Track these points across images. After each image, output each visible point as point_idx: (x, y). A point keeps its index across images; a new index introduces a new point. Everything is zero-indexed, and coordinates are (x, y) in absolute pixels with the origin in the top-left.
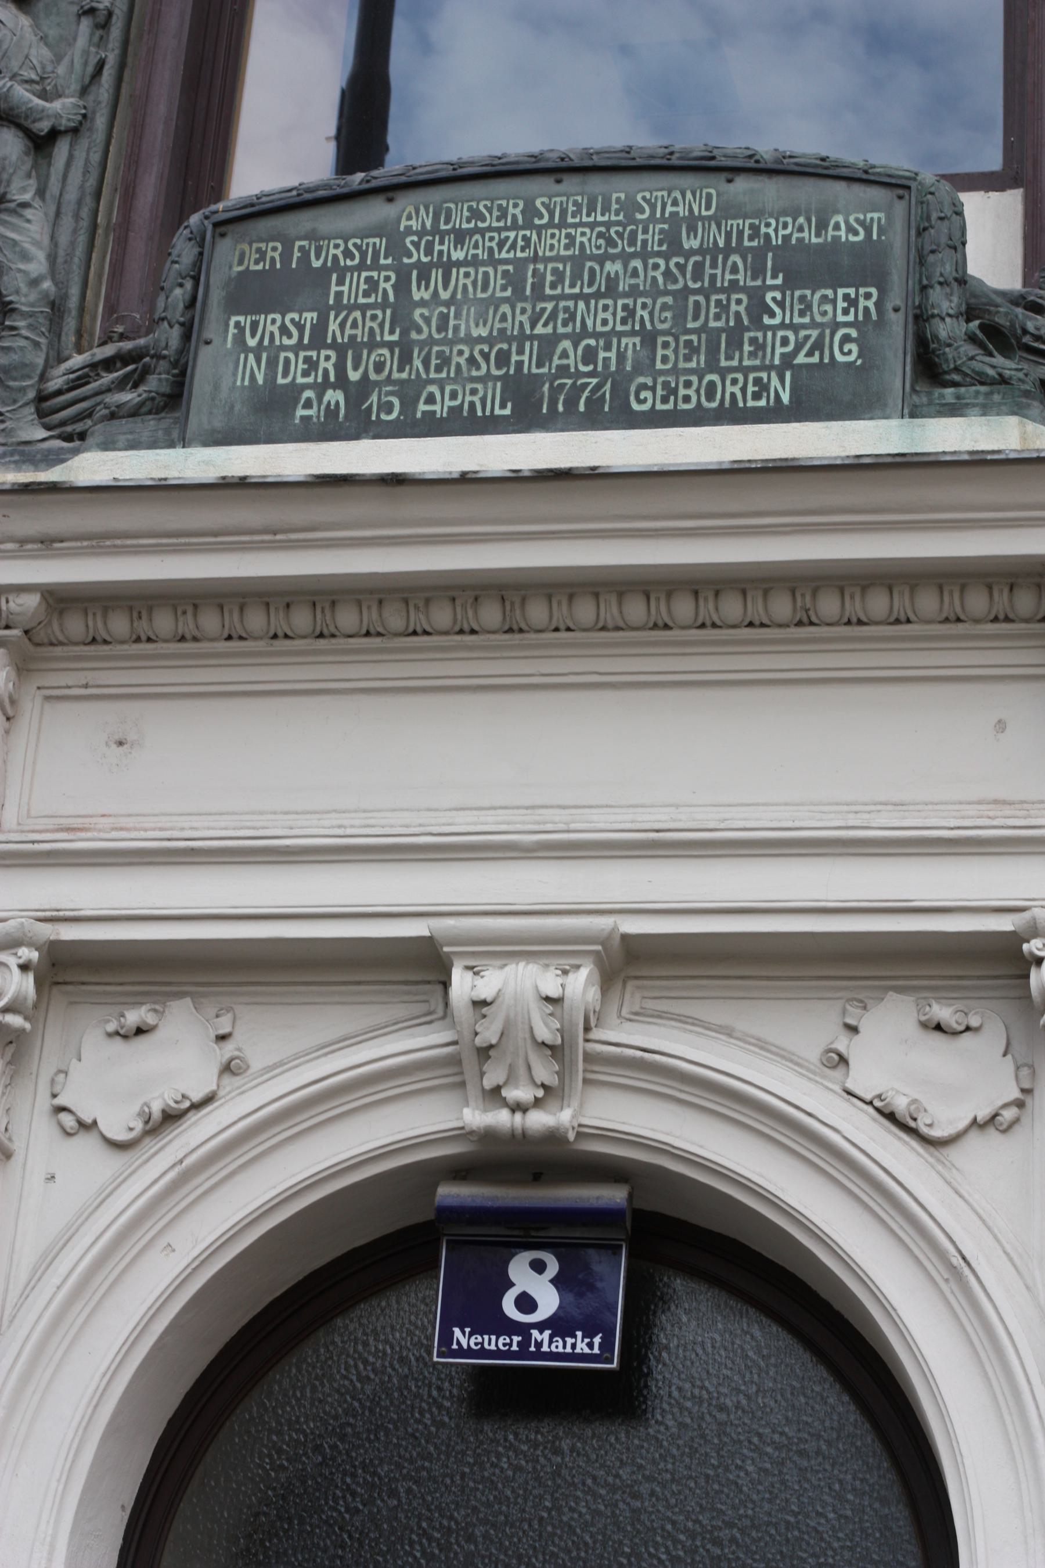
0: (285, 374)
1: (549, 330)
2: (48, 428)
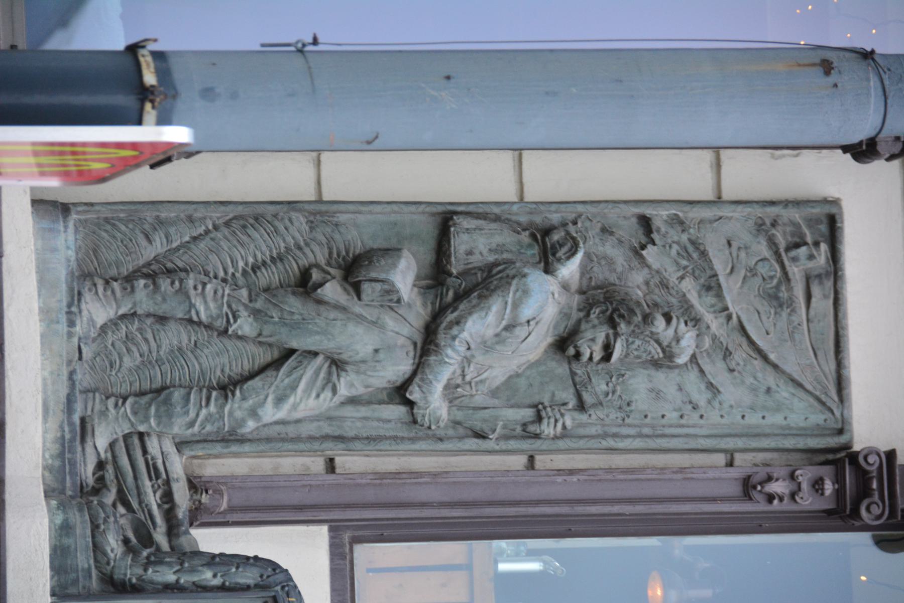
2: (112, 446)
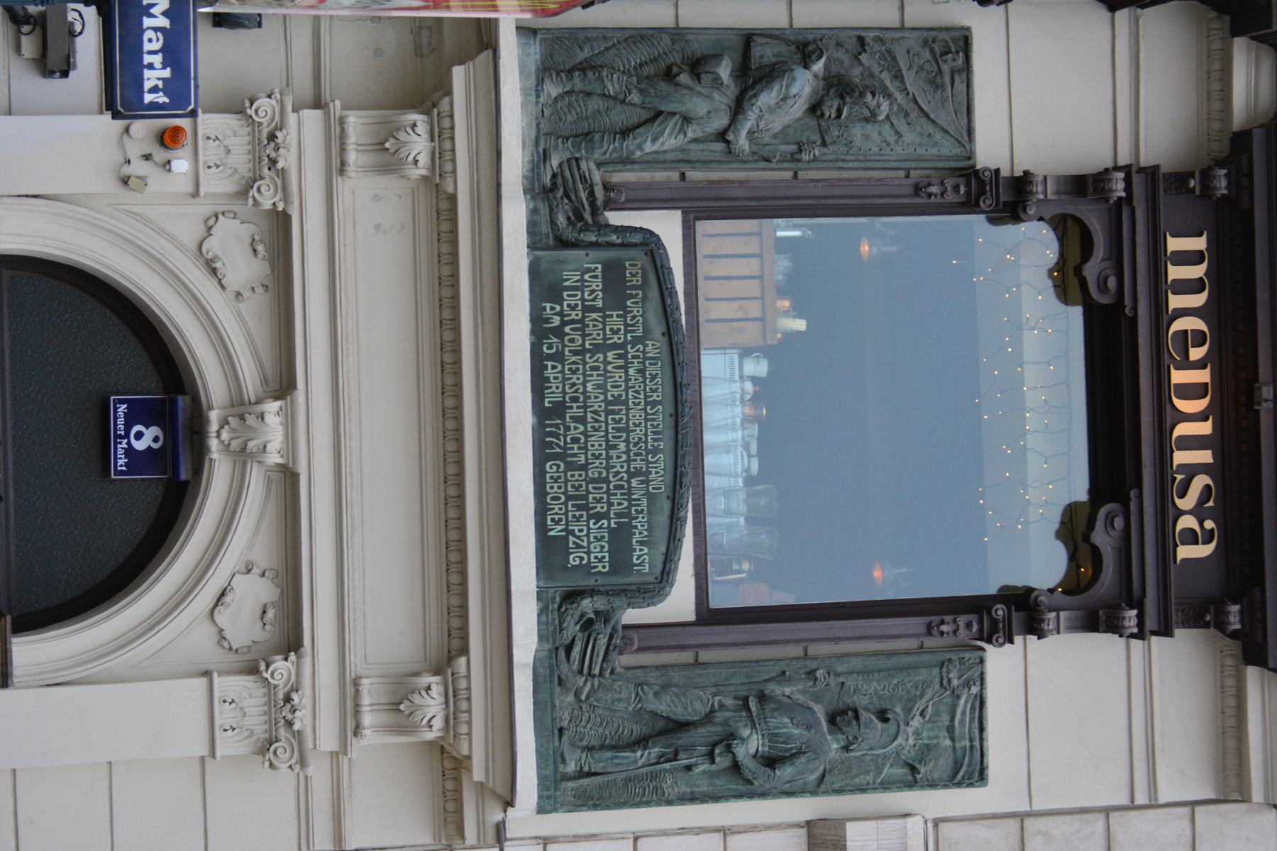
1: (589, 419)
2: (560, 165)
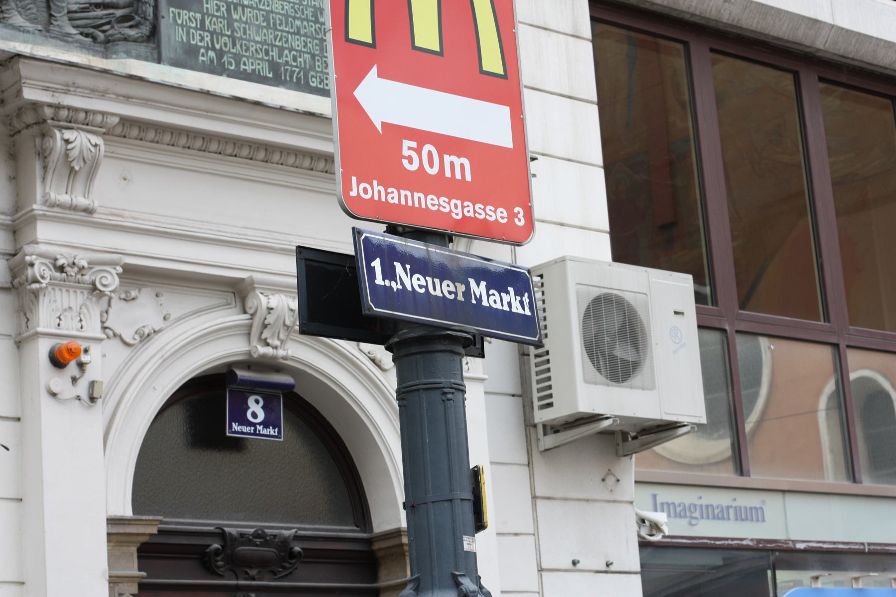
0: (193, 39)
